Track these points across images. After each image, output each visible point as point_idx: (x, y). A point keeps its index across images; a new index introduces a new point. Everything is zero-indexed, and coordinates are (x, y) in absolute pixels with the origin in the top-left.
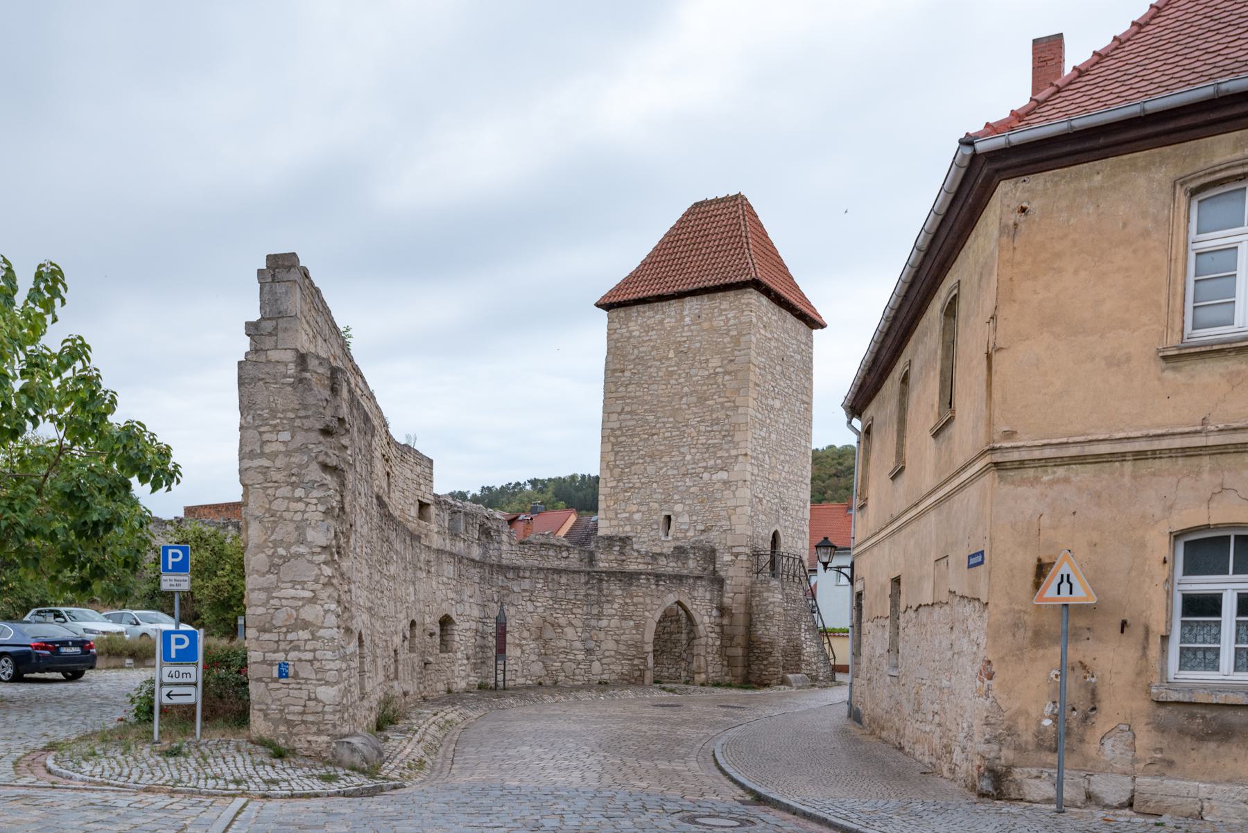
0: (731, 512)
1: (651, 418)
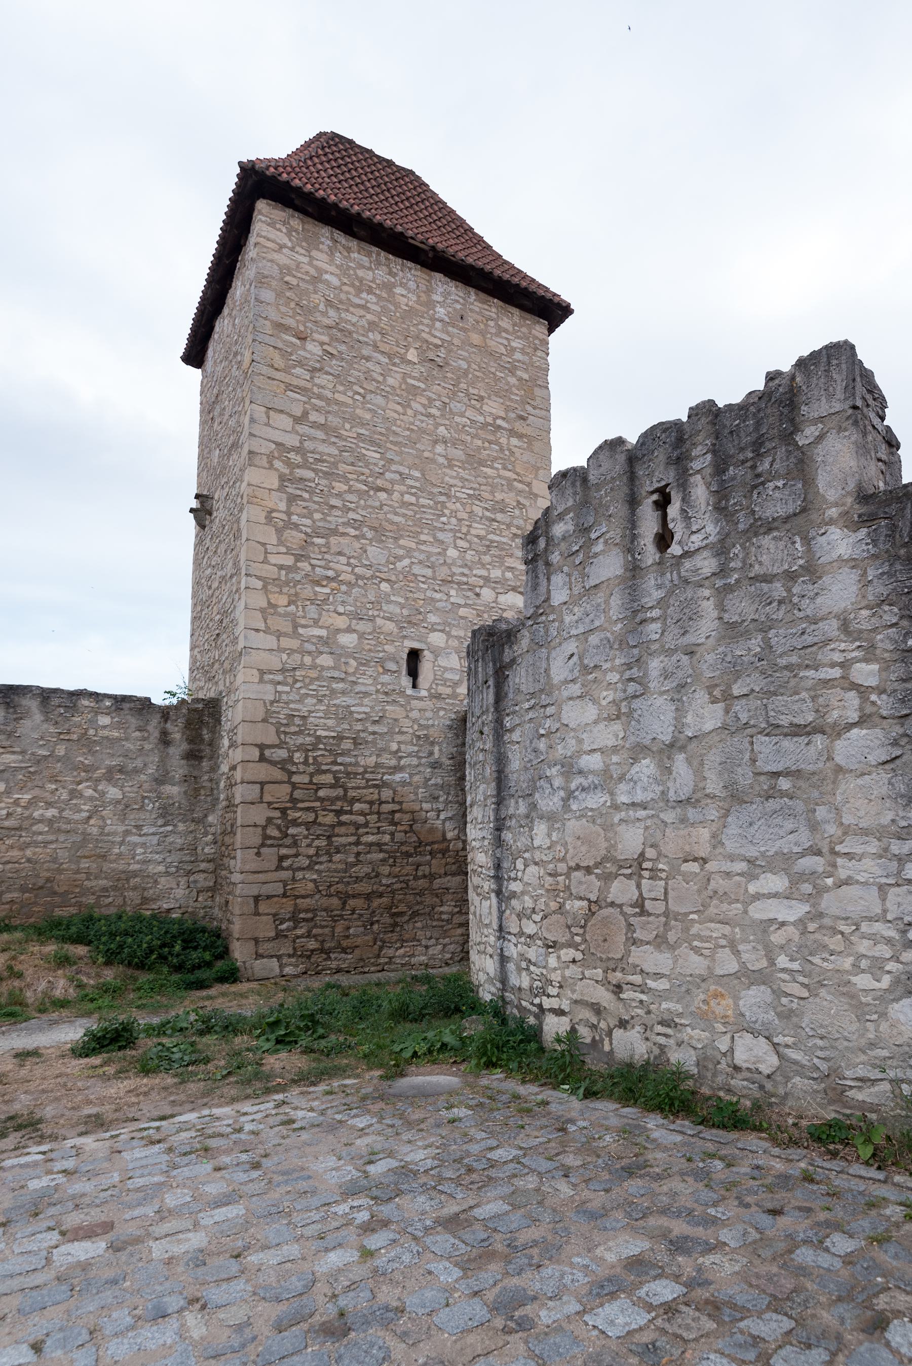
1: (373, 455)
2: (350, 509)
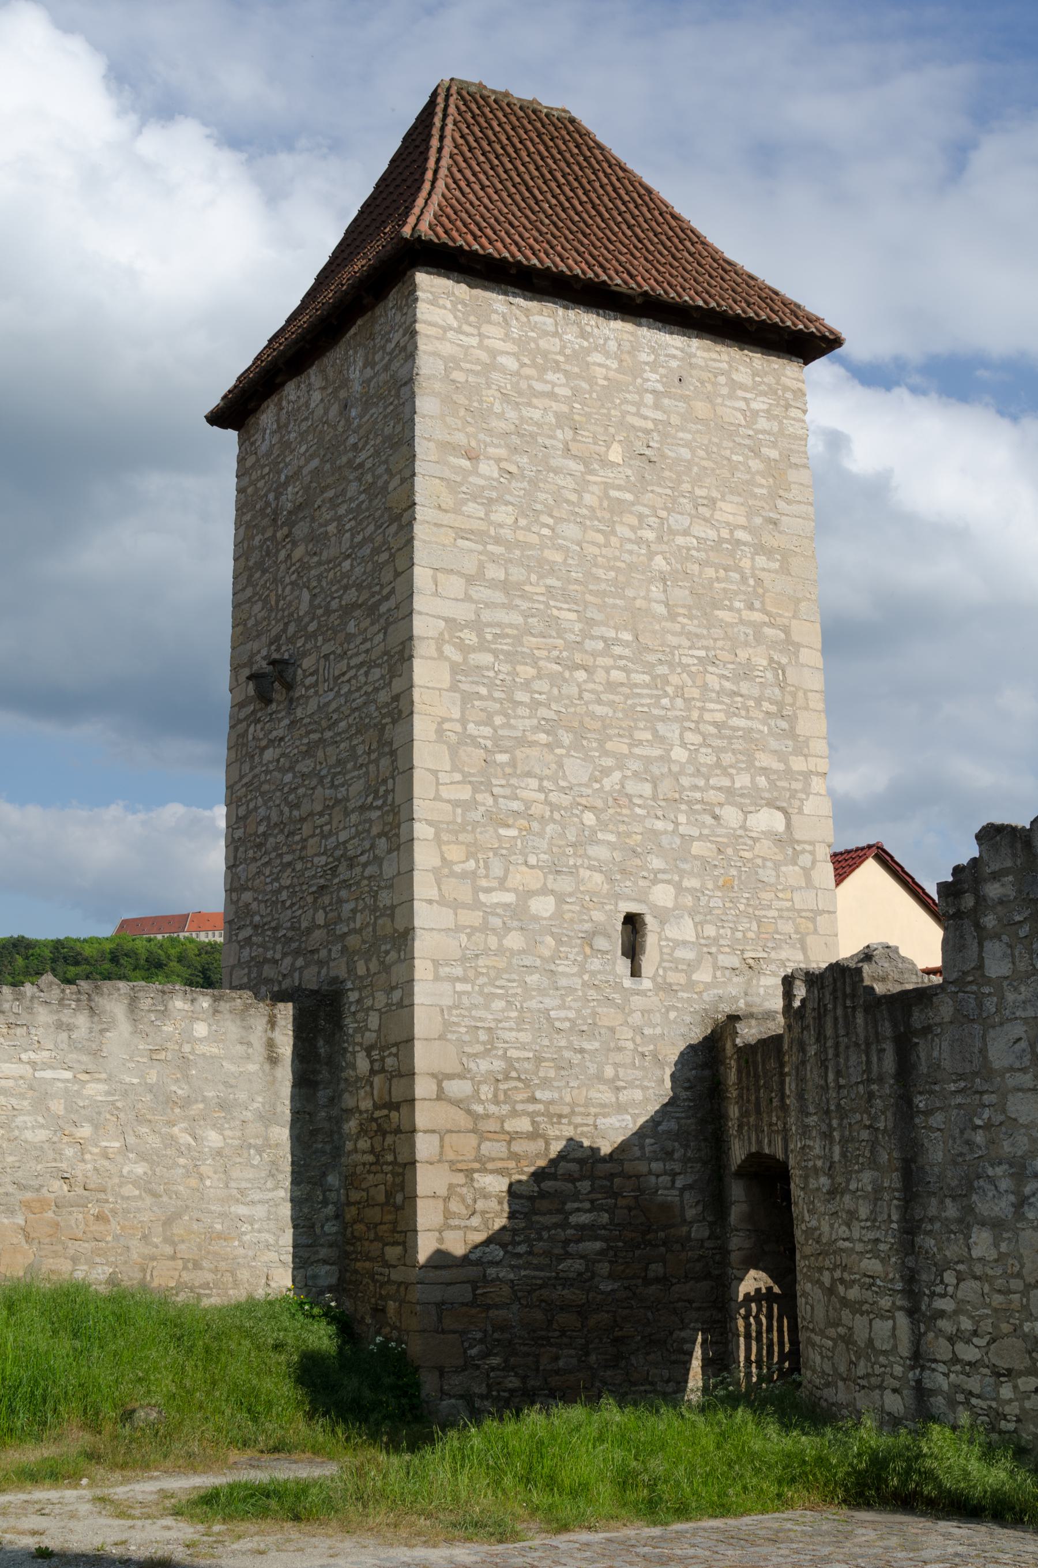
0: (805, 925)
2: (540, 704)
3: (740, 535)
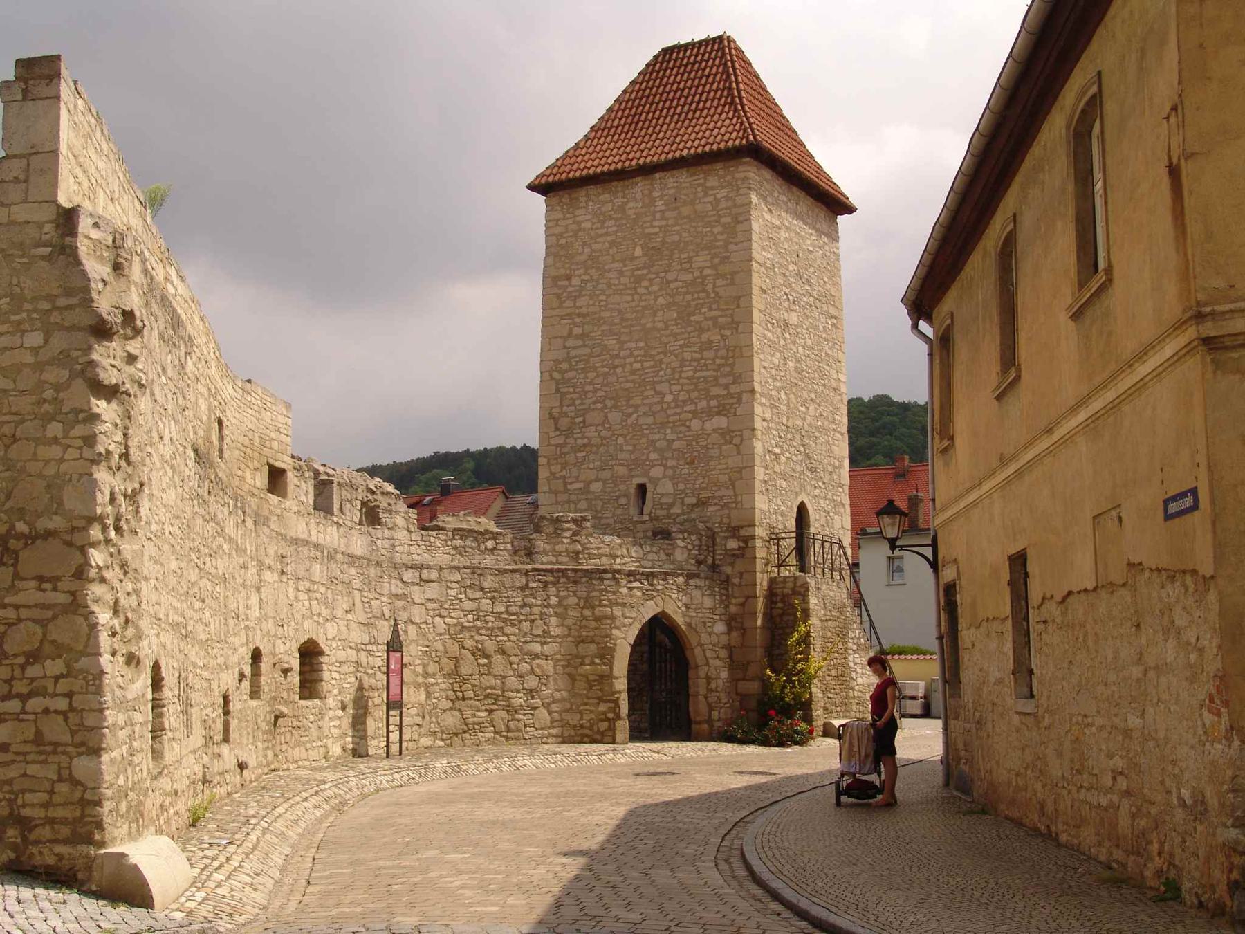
3: (706, 272)
